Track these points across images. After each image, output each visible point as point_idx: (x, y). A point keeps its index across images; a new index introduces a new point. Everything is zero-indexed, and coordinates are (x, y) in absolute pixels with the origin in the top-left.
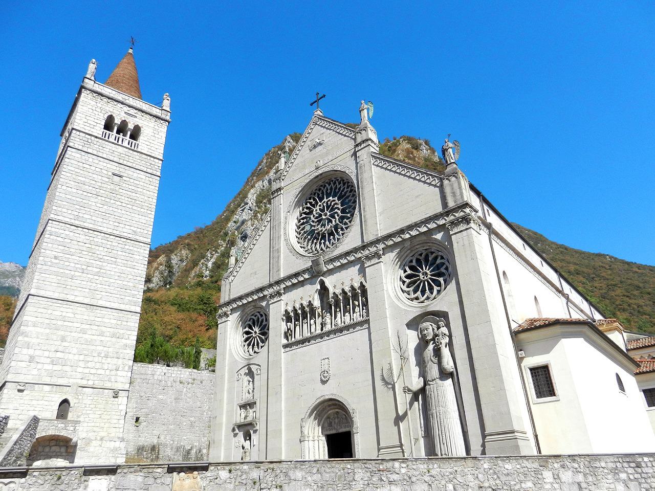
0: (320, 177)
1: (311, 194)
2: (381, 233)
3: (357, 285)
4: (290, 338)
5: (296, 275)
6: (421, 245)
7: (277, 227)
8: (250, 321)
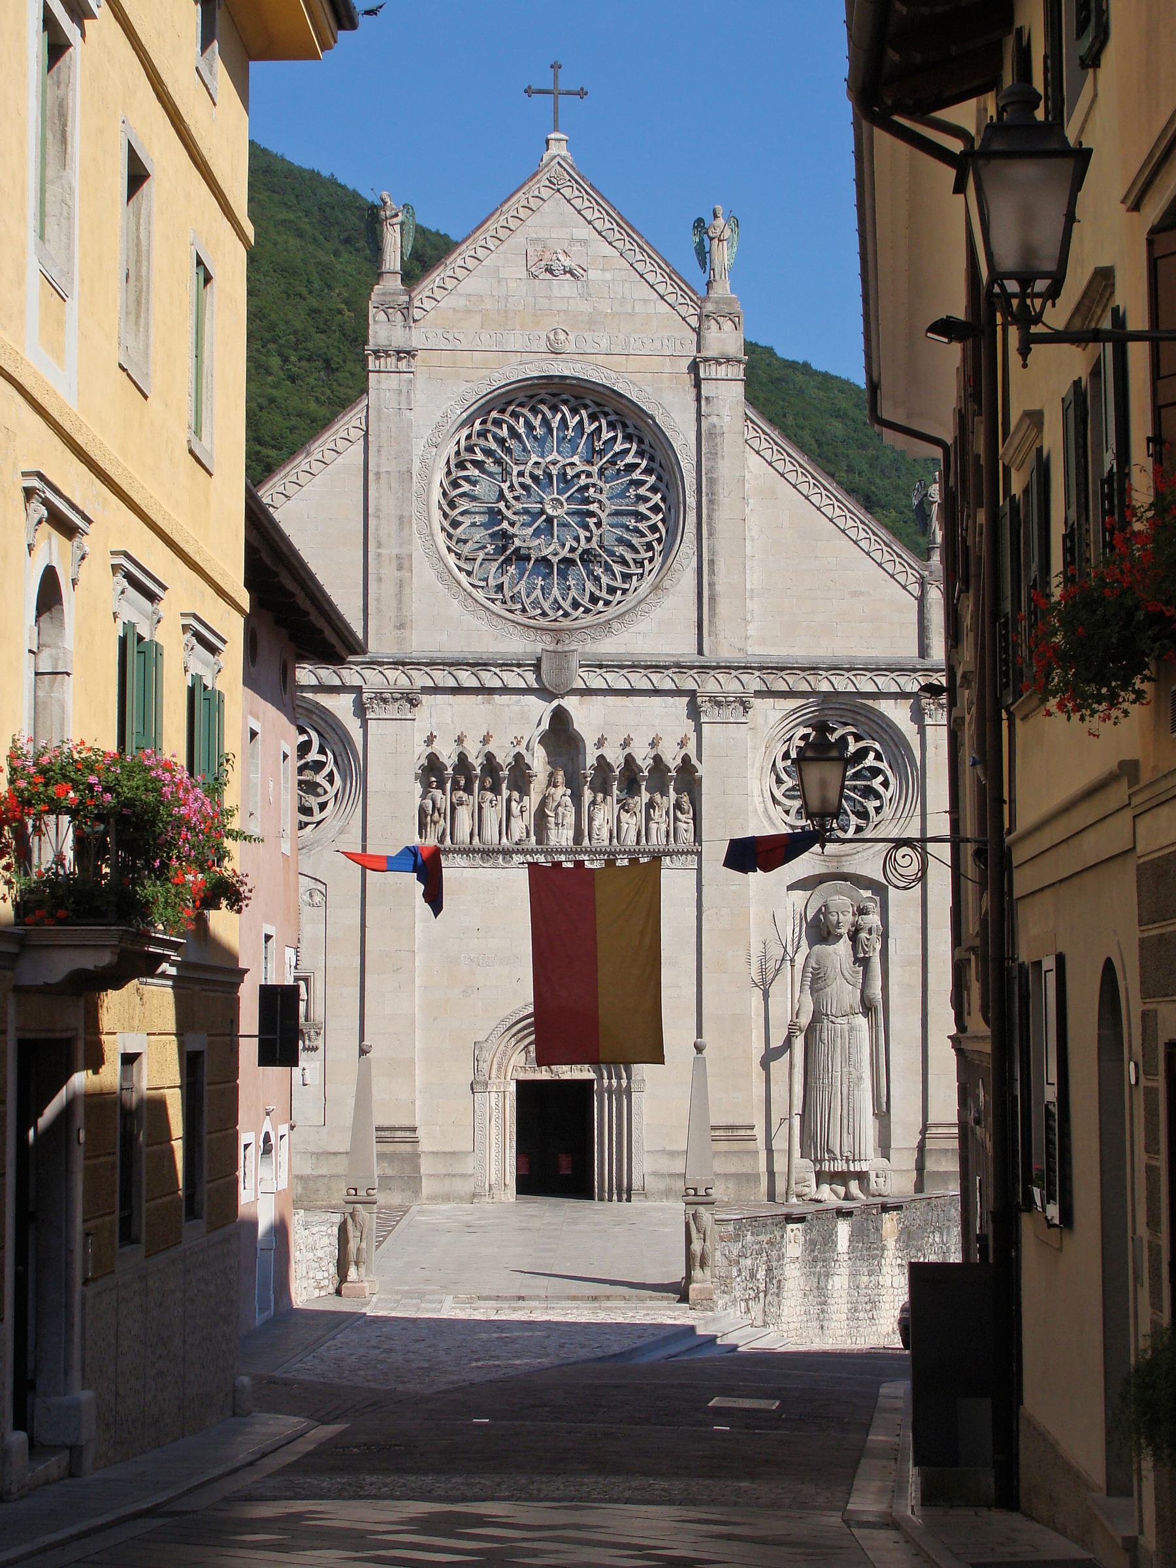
0: (556, 381)
2: (757, 650)
3: (672, 761)
6: (838, 712)
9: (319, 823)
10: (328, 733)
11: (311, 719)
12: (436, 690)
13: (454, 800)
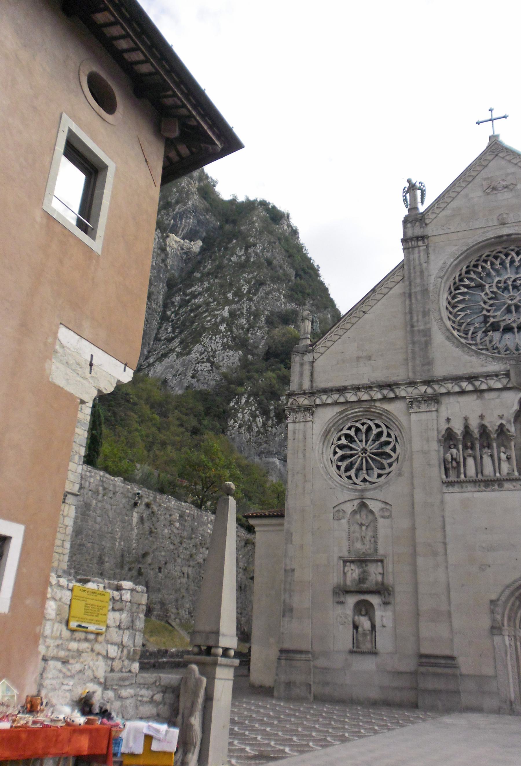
0: (505, 238)
1: (478, 260)
4: (451, 472)
5: (471, 378)
7: (419, 297)
8: (350, 428)
9: (389, 473)
10: (391, 425)
11: (381, 418)
12: (449, 394)
13: (465, 455)
